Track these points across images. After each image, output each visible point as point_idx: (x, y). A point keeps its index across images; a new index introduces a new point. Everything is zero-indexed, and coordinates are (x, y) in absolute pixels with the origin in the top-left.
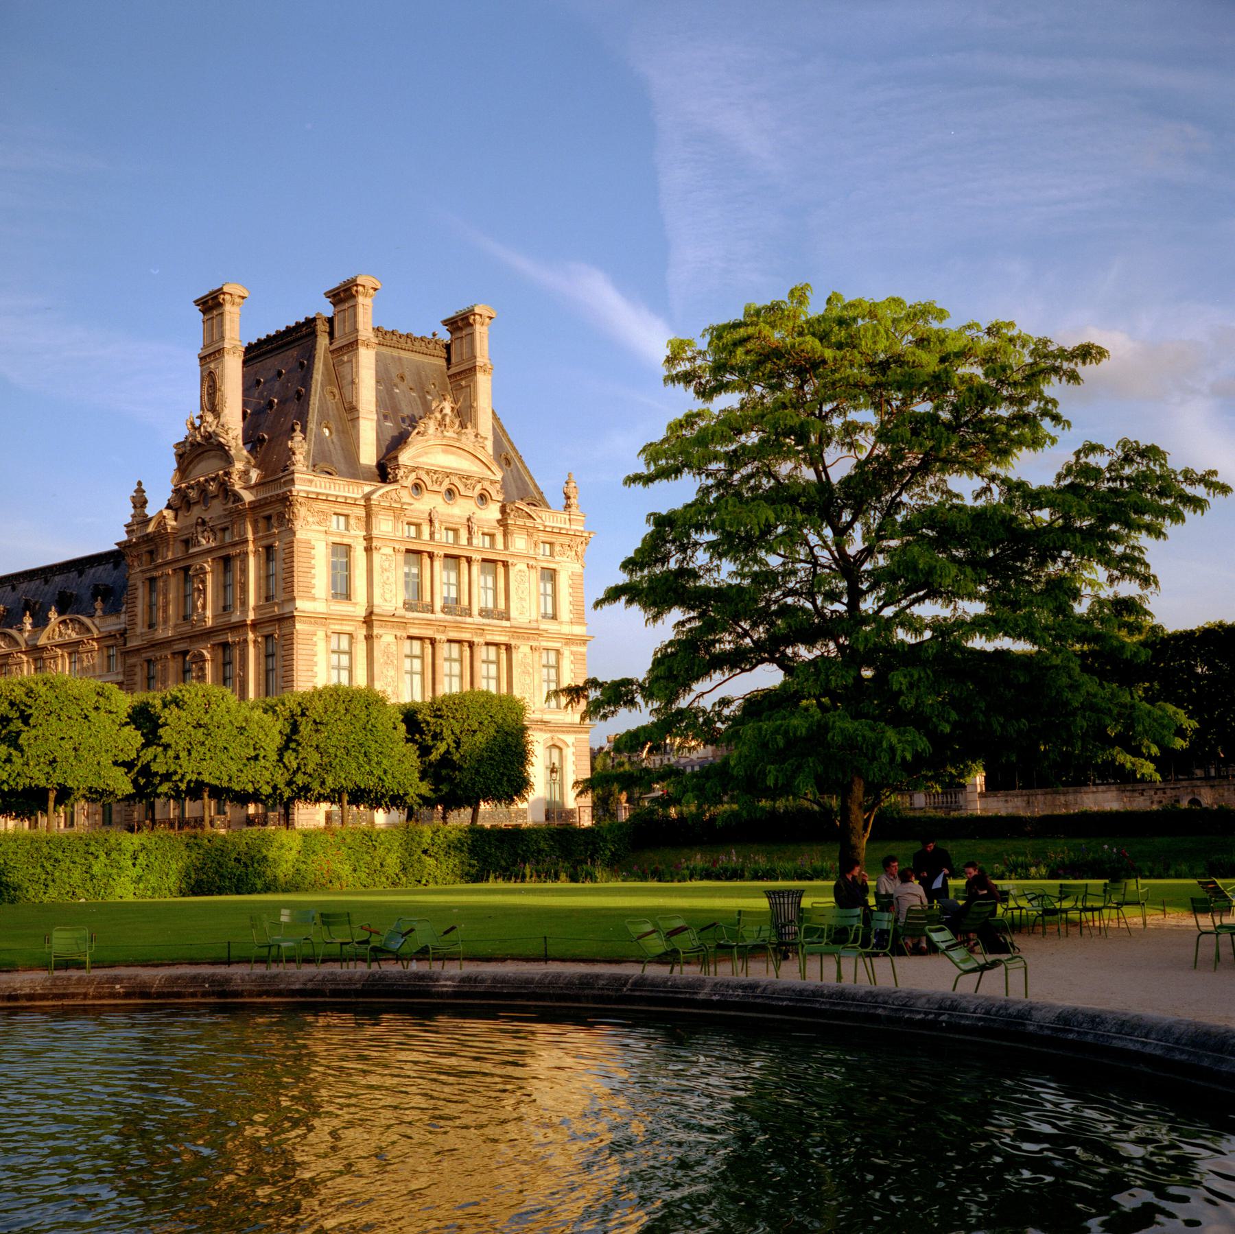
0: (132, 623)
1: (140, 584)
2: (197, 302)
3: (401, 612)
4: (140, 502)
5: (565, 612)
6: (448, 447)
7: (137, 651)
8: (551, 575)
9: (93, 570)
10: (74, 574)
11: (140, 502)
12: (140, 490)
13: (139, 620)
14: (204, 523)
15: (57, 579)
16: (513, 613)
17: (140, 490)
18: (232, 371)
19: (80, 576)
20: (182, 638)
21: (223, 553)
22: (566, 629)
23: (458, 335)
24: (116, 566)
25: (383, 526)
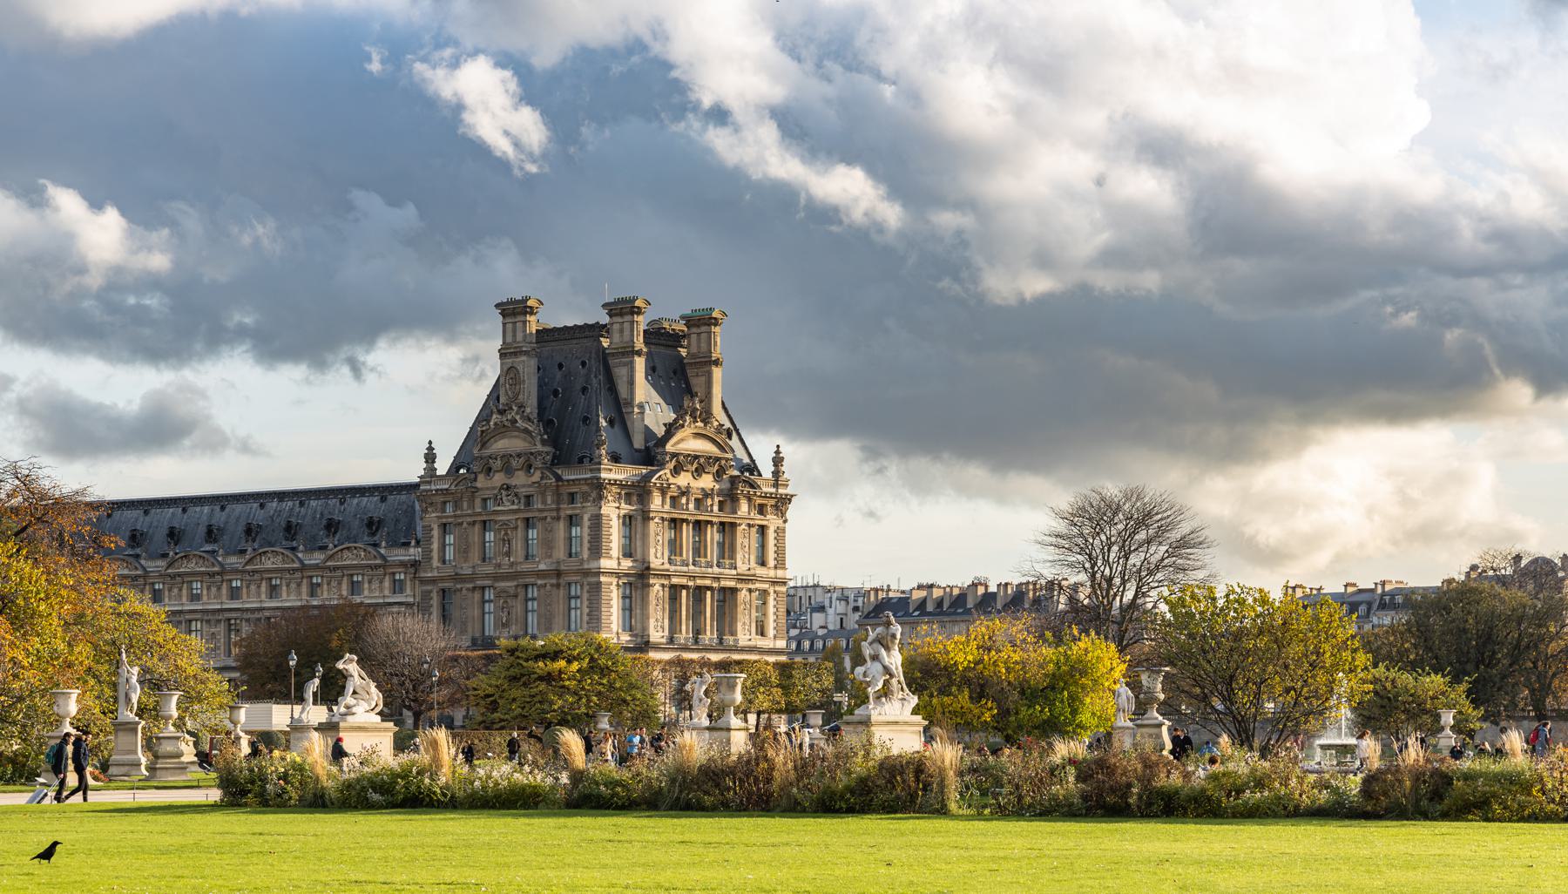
0: (427, 556)
1: (435, 527)
2: (497, 306)
3: (667, 566)
4: (430, 457)
5: (772, 563)
6: (698, 435)
7: (433, 581)
8: (762, 530)
9: (355, 501)
10: (333, 502)
11: (430, 457)
12: (430, 448)
13: (435, 555)
14: (508, 488)
15: (313, 503)
16: (739, 564)
17: (430, 448)
18: (528, 367)
19: (342, 504)
20: (487, 576)
21: (530, 515)
22: (772, 573)
23: (694, 330)
24: (383, 499)
25: (656, 502)
